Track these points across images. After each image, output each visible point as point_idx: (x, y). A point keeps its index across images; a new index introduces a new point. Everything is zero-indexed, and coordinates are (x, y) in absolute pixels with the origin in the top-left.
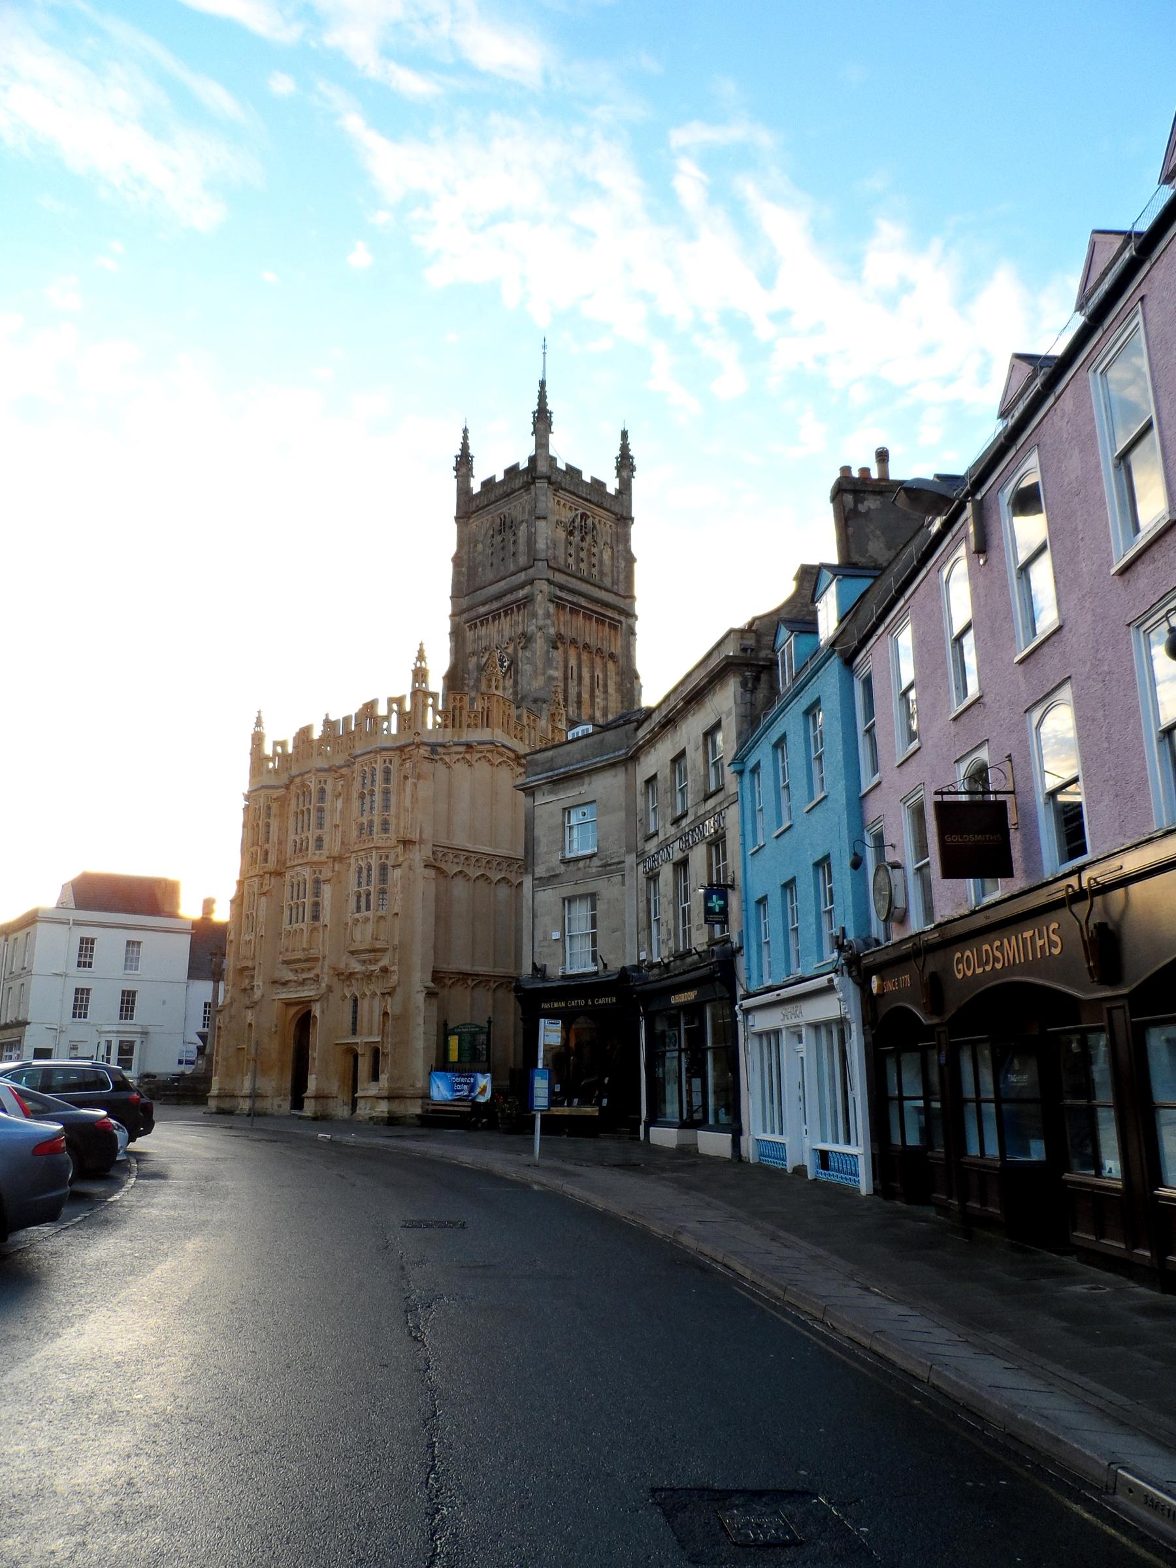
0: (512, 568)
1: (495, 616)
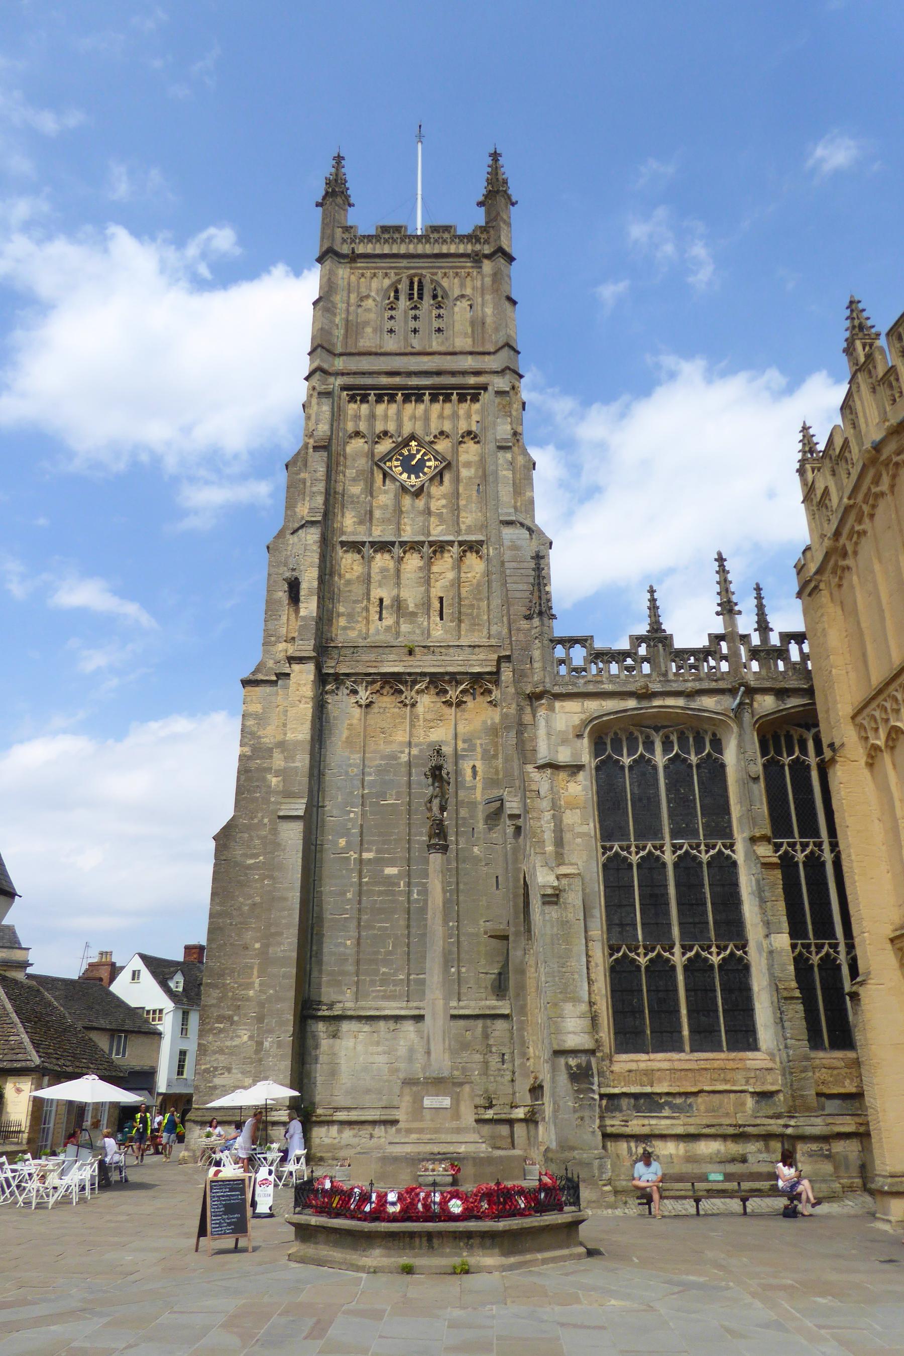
0: (435, 347)
1: (413, 395)
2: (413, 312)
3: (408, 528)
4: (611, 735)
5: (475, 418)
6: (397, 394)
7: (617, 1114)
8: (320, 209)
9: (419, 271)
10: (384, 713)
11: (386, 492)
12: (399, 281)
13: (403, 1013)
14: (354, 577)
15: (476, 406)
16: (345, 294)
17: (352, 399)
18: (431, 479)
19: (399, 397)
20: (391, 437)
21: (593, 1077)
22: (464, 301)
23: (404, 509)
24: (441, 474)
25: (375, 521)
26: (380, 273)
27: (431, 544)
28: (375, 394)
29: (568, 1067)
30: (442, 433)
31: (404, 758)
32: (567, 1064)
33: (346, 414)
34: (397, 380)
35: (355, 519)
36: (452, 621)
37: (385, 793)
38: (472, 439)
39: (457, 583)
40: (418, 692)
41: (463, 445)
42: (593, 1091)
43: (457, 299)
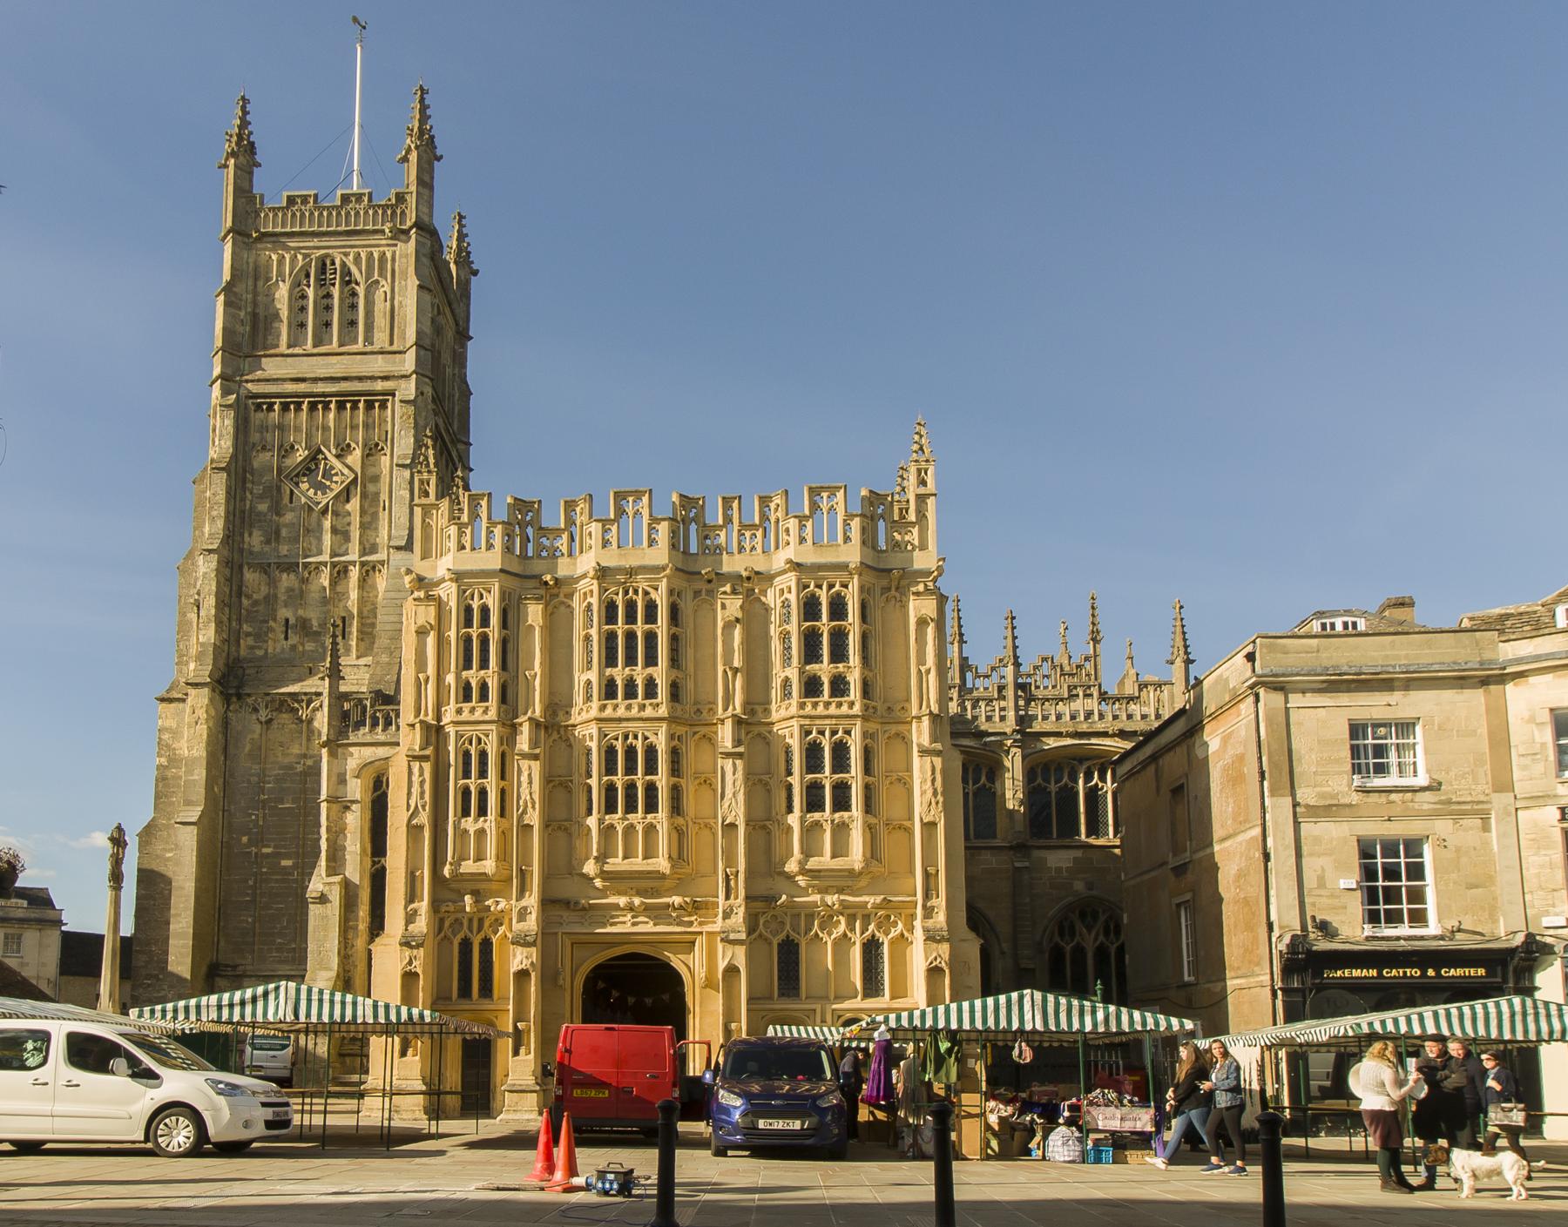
14: (261, 597)
25: (281, 540)
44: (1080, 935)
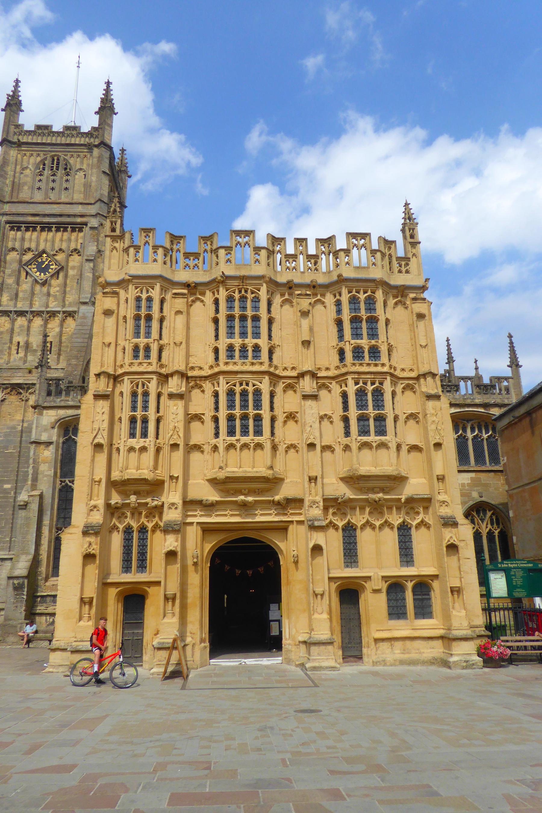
0: (63, 199)
1: (46, 227)
2: (52, 178)
3: (37, 303)
4: (73, 426)
5: (80, 241)
6: (37, 227)
7: (44, 604)
8: (4, 113)
9: (57, 153)
10: (11, 404)
11: (26, 283)
12: (46, 159)
13: (5, 557)
15: (81, 234)
16: (13, 166)
17: (12, 229)
18: (52, 276)
19: (38, 228)
20: (32, 251)
21: (24, 588)
22: (81, 172)
23: (35, 292)
24: (58, 273)
25: (19, 299)
26: (35, 154)
27: (48, 312)
28: (25, 226)
29: (14, 584)
30: (60, 250)
31: (19, 428)
32: (13, 583)
33: (8, 237)
34: (37, 219)
35: (8, 298)
36: (55, 355)
37: (8, 447)
38: (77, 253)
39: (61, 334)
40: (30, 394)
41: (72, 257)
42: (23, 595)
43: (77, 171)
44: (478, 525)
